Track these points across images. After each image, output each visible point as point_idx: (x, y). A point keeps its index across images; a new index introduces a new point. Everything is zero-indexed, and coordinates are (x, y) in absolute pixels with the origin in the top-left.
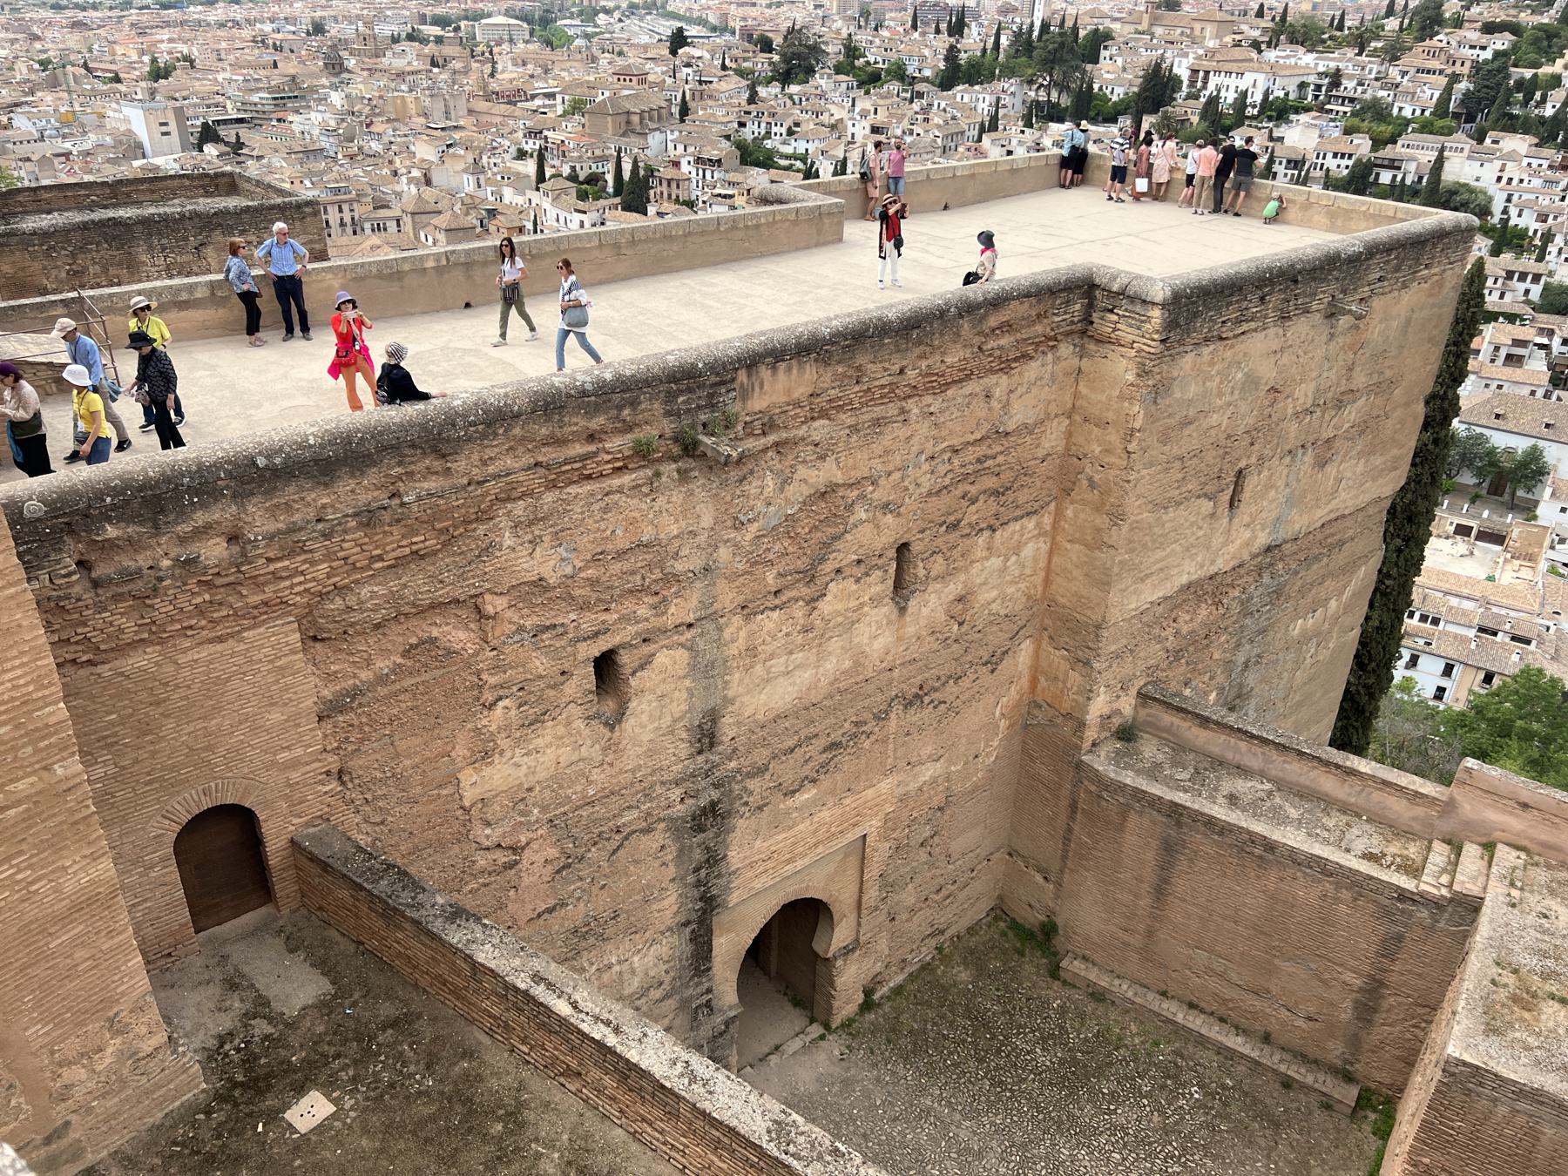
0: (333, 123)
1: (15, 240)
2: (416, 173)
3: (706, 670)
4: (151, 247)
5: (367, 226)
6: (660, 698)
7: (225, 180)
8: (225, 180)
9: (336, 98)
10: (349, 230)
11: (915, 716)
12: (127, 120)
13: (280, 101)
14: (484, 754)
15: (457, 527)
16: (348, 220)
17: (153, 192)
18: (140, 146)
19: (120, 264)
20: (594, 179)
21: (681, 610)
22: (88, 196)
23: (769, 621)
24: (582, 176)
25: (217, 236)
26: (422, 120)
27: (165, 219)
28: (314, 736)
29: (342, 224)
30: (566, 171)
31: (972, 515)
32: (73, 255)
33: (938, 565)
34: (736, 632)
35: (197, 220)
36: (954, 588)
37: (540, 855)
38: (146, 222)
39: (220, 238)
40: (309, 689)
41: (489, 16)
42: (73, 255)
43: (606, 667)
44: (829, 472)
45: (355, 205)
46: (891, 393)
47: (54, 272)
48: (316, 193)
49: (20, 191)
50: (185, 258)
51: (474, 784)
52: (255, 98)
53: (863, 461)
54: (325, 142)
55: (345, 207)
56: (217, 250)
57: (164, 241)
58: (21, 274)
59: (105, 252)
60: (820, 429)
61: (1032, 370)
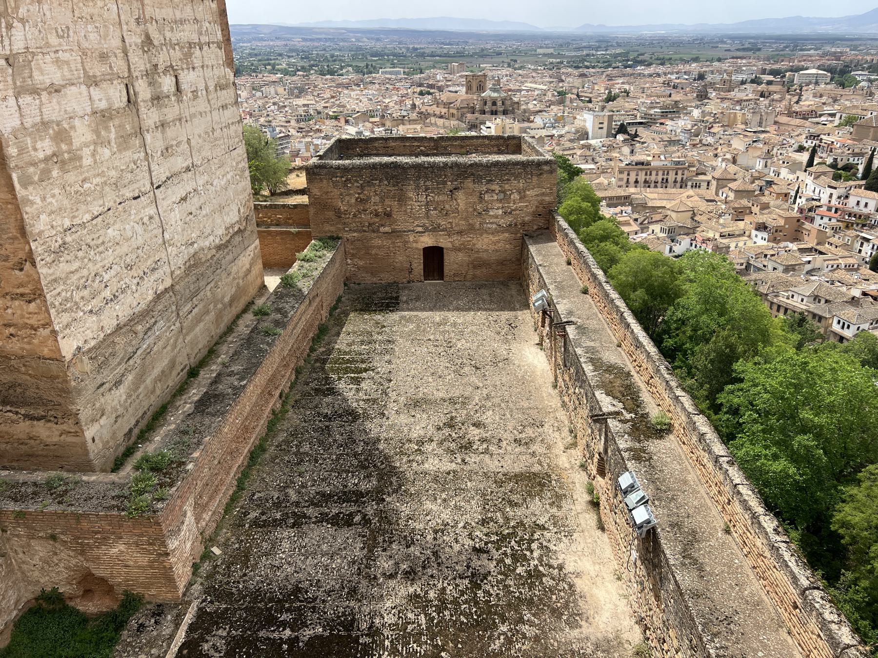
0: (689, 127)
1: (325, 171)
2: (728, 156)
4: (418, 187)
5: (690, 184)
7: (515, 142)
8: (515, 142)
9: (696, 113)
10: (678, 185)
12: (585, 121)
13: (665, 114)
16: (679, 179)
17: (462, 147)
18: (587, 133)
19: (394, 197)
20: (848, 168)
22: (419, 147)
24: (840, 165)
25: (469, 183)
26: (743, 127)
27: (433, 166)
29: (675, 182)
30: (829, 160)
32: (362, 187)
35: (455, 169)
38: (417, 167)
39: (471, 185)
41: (807, 69)
42: (362, 187)
45: (686, 172)
47: (347, 198)
48: (665, 163)
49: (376, 139)
50: (441, 198)
52: (652, 112)
54: (682, 137)
55: (680, 172)
56: (466, 194)
57: (428, 183)
58: (325, 196)
59: (386, 187)
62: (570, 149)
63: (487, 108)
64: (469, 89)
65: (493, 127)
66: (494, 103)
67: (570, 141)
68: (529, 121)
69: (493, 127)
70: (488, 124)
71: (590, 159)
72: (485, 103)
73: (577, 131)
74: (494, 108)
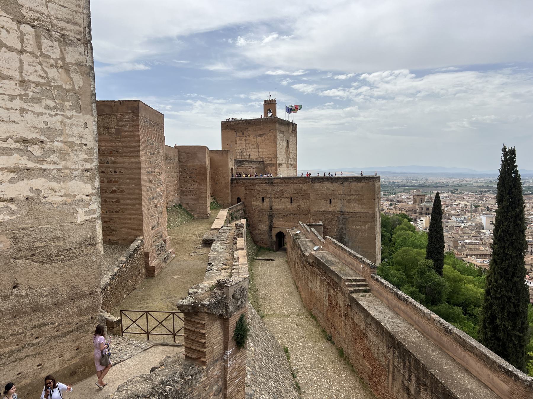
3: (271, 202)
6: (267, 203)
11: (294, 216)
12: (481, 220)
14: (254, 201)
15: (253, 185)
21: (269, 196)
23: (277, 200)
28: (244, 195)
31: (299, 197)
33: (295, 201)
34: (274, 200)
36: (298, 204)
37: (257, 212)
40: (244, 192)
43: (263, 198)
44: (282, 188)
46: (288, 183)
51: (253, 203)
53: (286, 188)
60: (281, 185)
61: (305, 185)
62: (468, 233)
63: (423, 212)
64: (415, 201)
65: (424, 220)
66: (428, 209)
67: (472, 230)
68: (449, 219)
69: (424, 220)
70: (422, 219)
71: (479, 238)
72: (423, 209)
73: (476, 225)
74: (428, 212)
